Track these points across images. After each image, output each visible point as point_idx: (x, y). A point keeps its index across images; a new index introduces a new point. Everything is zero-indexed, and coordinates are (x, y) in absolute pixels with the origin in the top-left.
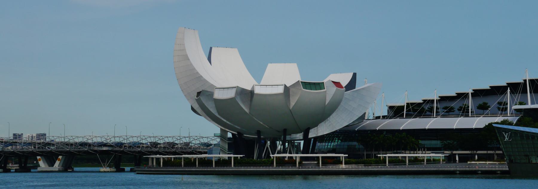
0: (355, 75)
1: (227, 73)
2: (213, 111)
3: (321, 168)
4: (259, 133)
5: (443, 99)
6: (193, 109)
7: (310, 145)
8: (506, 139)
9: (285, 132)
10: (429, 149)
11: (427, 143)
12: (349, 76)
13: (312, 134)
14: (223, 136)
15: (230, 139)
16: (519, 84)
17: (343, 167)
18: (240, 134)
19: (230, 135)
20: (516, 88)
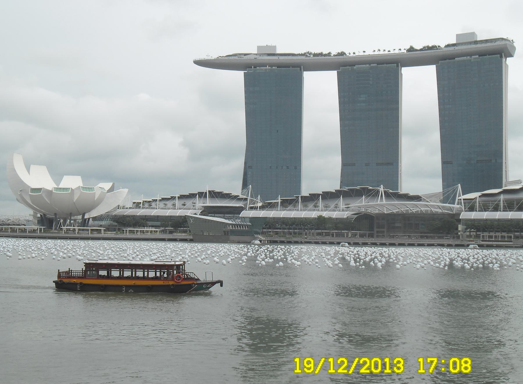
1: (39, 179)
2: (29, 201)
3: (90, 235)
4: (55, 214)
5: (163, 199)
6: (17, 200)
7: (85, 222)
9: (71, 215)
10: (152, 226)
13: (86, 216)
14: (34, 216)
15: (38, 217)
17: (102, 235)
18: (44, 215)
19: (39, 215)
20: (202, 195)
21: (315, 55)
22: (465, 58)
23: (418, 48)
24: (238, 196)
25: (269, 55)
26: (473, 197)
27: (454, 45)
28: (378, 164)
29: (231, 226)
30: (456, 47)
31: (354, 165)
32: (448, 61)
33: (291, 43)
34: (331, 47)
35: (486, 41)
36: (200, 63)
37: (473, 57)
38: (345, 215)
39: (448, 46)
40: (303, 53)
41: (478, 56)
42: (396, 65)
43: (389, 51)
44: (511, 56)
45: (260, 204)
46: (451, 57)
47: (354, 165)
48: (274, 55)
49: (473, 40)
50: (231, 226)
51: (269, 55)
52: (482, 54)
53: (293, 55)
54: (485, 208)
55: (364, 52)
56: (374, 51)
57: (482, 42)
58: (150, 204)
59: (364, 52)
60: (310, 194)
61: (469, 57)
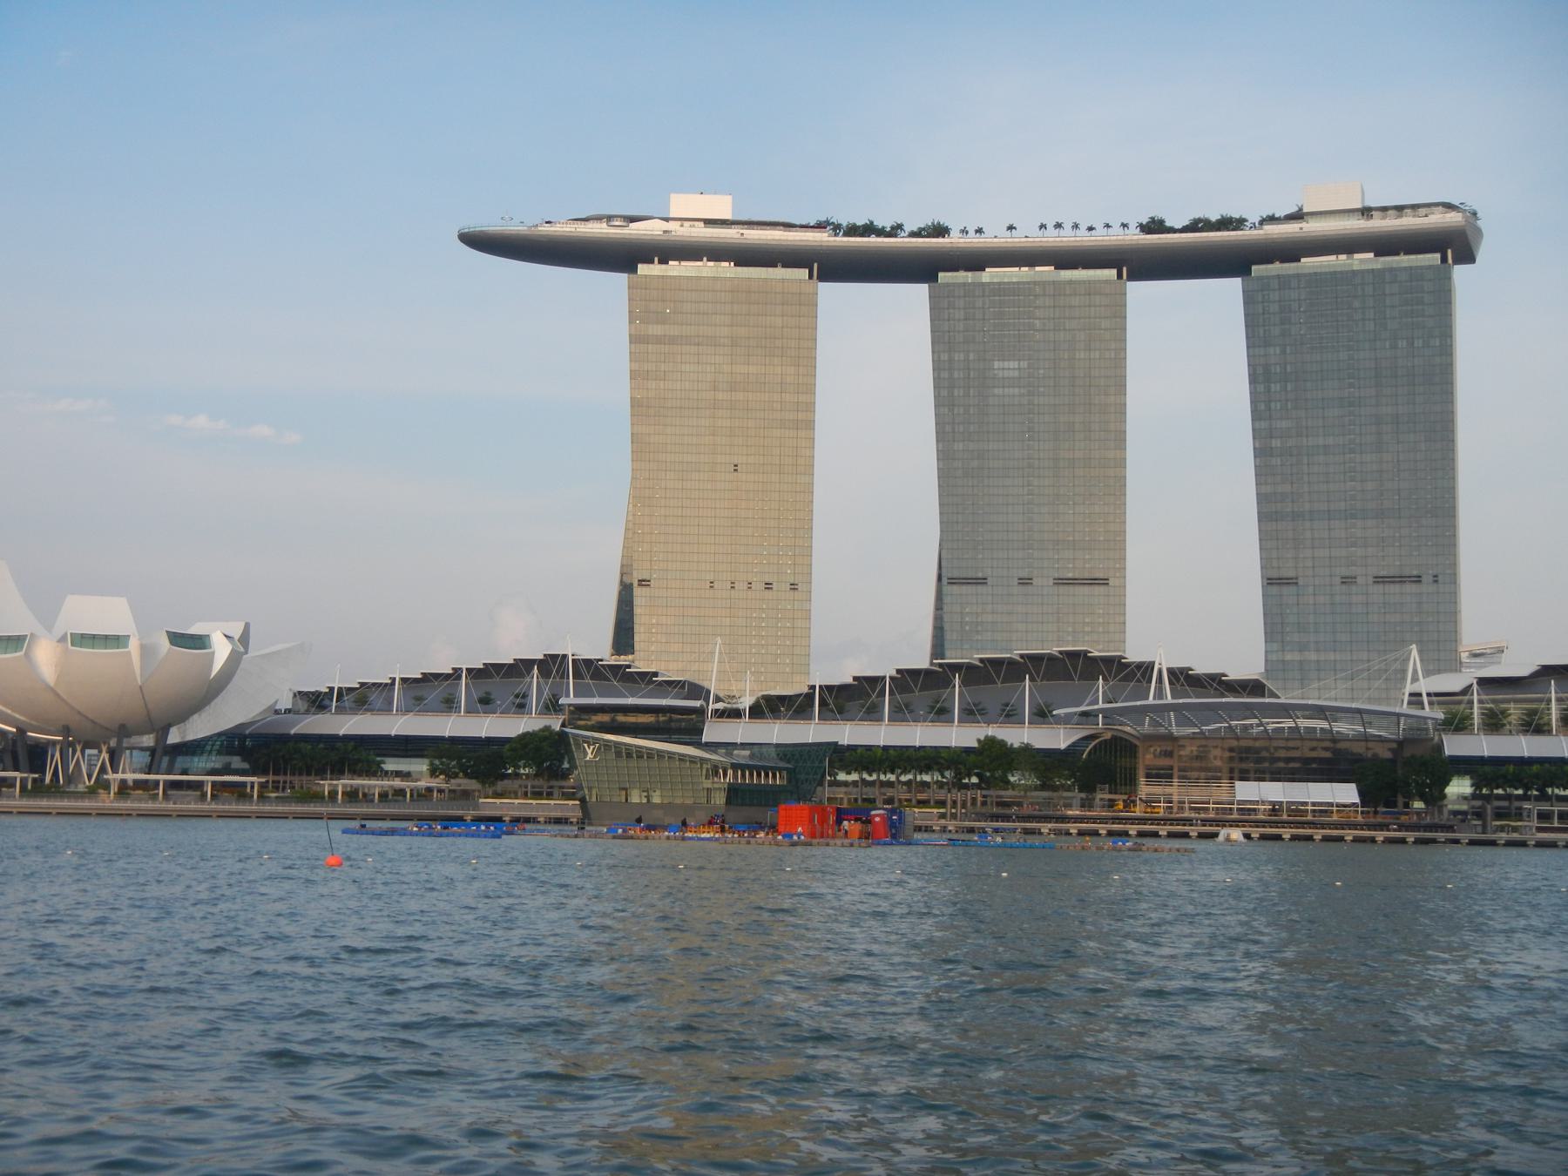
0: (247, 626)
8: (589, 756)
11: (391, 765)
12: (241, 626)
16: (554, 657)
22: (1333, 258)
23: (1178, 226)
24: (655, 674)
25: (709, 222)
26: (1457, 688)
27: (1298, 216)
28: (1061, 582)
29: (730, 772)
30: (1304, 225)
31: (982, 581)
32: (1277, 265)
34: (902, 206)
35: (1400, 209)
36: (479, 242)
37: (1357, 256)
38: (1057, 738)
39: (1271, 219)
41: (1371, 255)
42: (1114, 272)
43: (1091, 229)
45: (746, 702)
46: (1290, 251)
47: (982, 581)
49: (1359, 206)
50: (730, 772)
52: (1385, 245)
53: (788, 226)
54: (1494, 723)
55: (1011, 228)
56: (1043, 226)
58: (362, 697)
59: (1011, 228)
60: (899, 671)
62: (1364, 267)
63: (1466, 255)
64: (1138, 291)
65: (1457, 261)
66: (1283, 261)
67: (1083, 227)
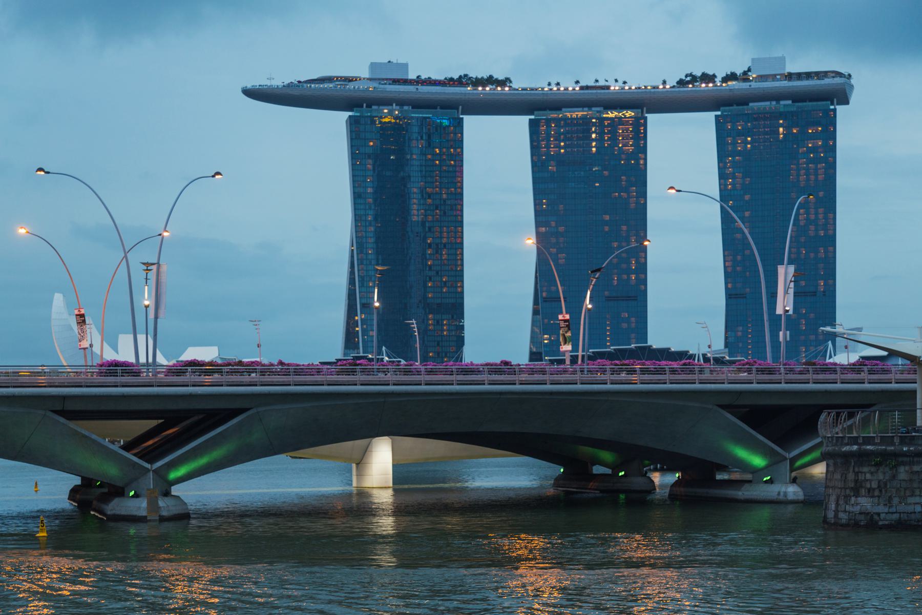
21: (478, 82)
22: (768, 103)
27: (745, 76)
32: (735, 107)
33: (432, 58)
35: (809, 75)
37: (782, 102)
40: (456, 77)
41: (790, 102)
44: (847, 103)
46: (742, 100)
48: (406, 82)
51: (396, 81)
52: (798, 97)
55: (577, 82)
57: (799, 76)
59: (577, 82)
61: (774, 103)
62: (786, 110)
63: (845, 101)
64: (653, 119)
65: (838, 104)
66: (738, 105)
67: (620, 83)
